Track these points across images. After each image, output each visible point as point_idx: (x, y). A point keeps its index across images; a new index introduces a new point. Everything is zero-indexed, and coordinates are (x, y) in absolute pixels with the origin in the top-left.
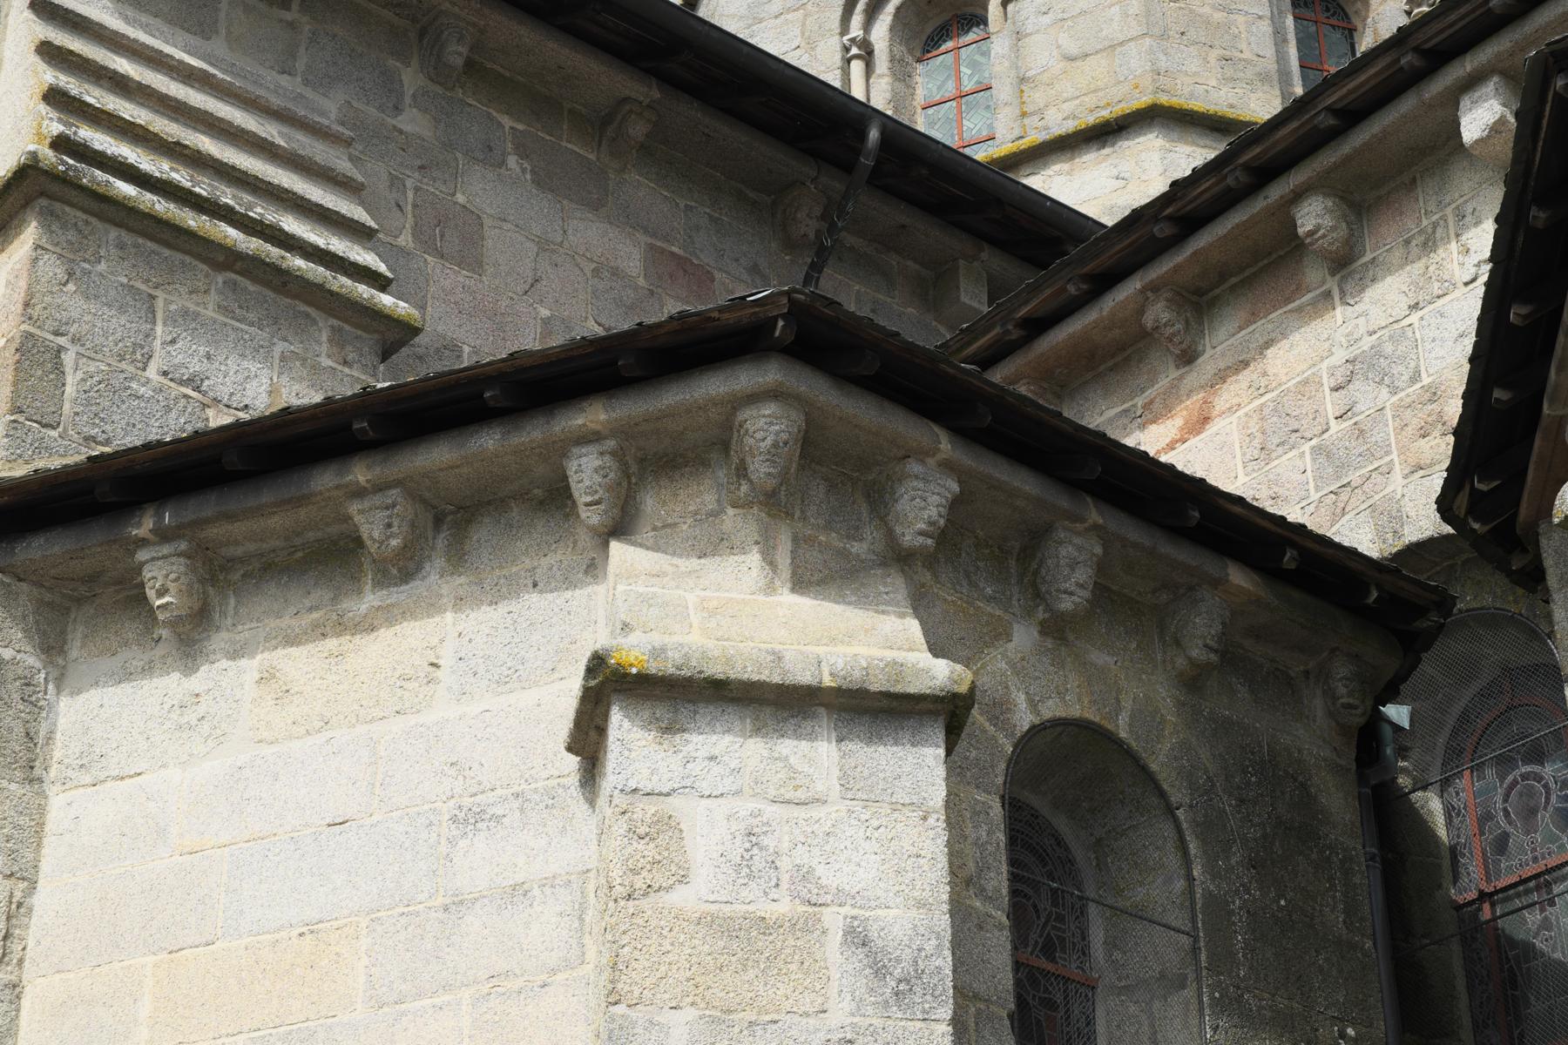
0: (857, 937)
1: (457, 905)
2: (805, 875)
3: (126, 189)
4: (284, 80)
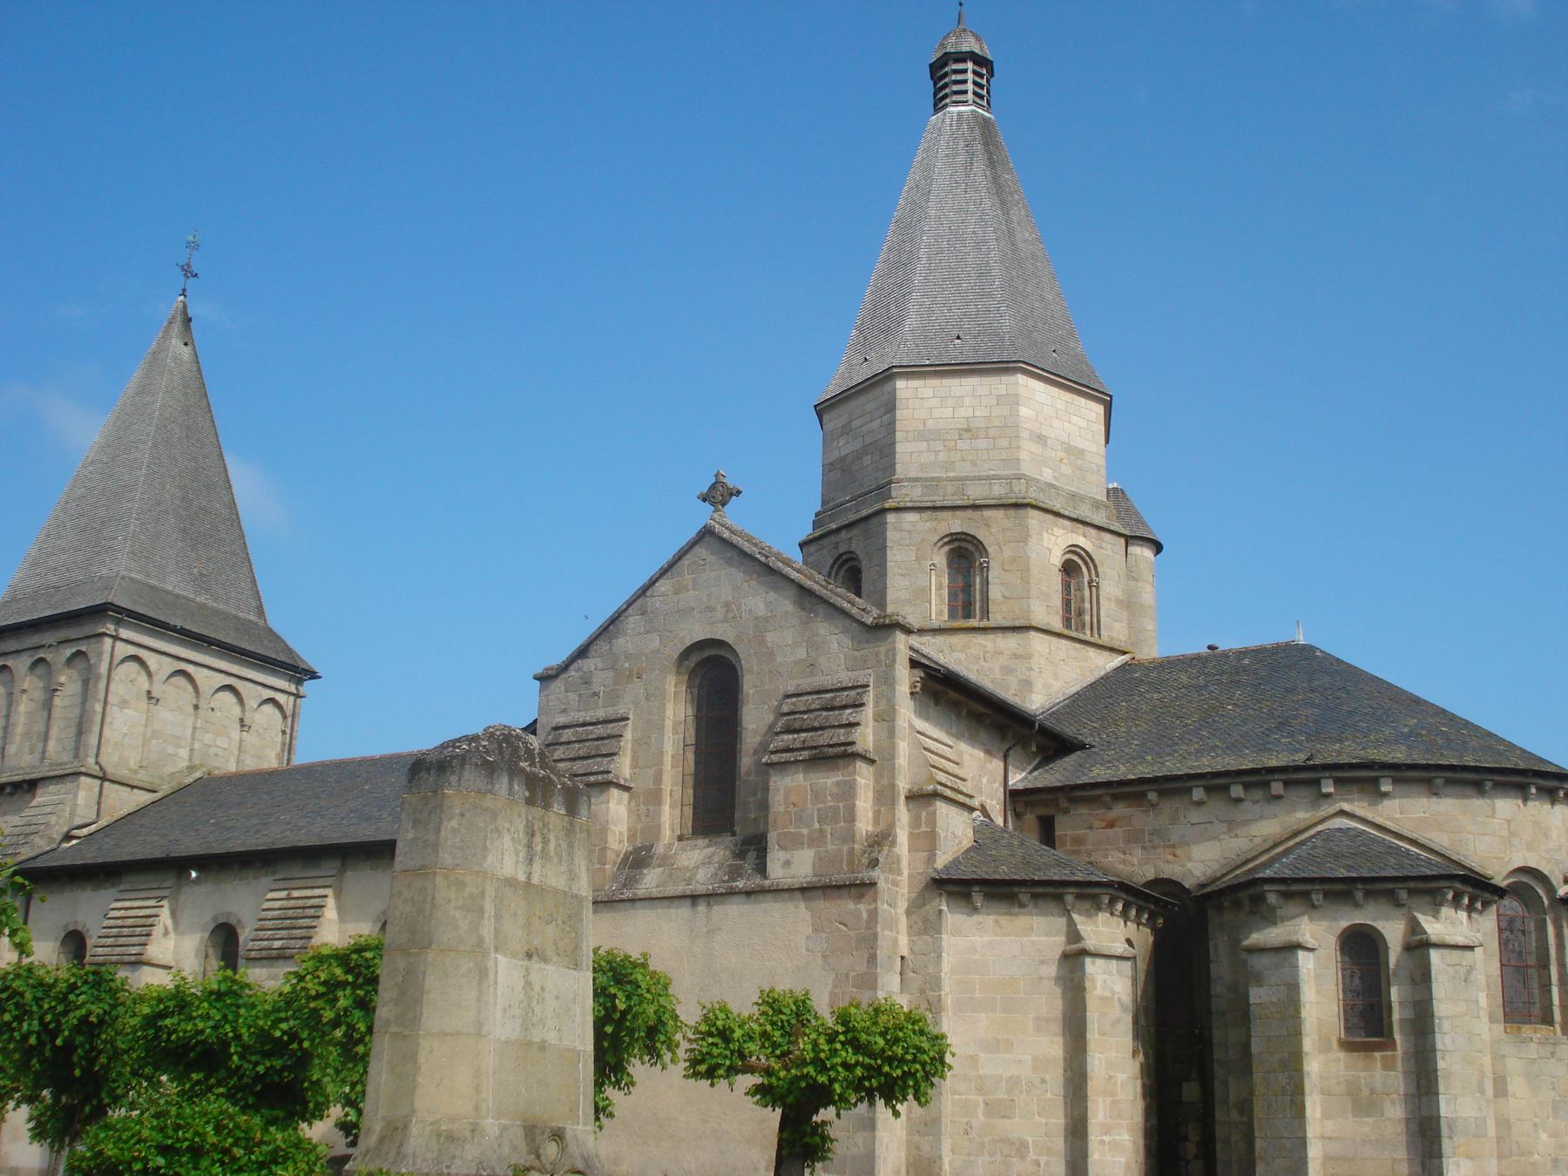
0: (1119, 1000)
1: (1041, 978)
2: (1112, 989)
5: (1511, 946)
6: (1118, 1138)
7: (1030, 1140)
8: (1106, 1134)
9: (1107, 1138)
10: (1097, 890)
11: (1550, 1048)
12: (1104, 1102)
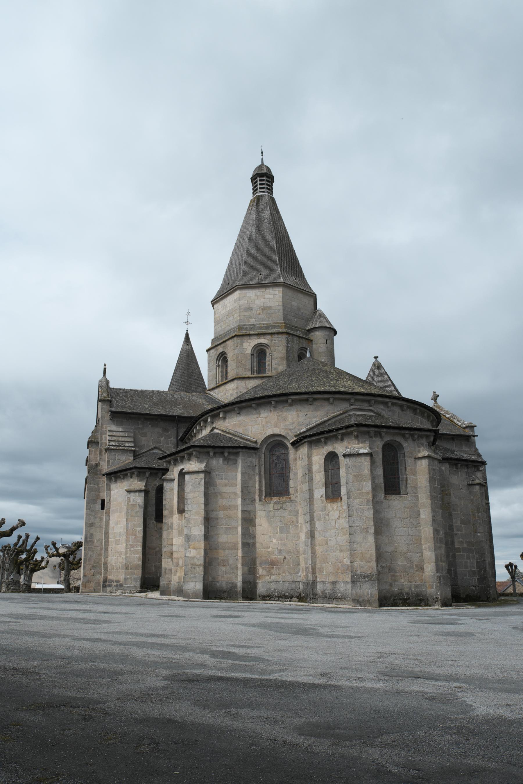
0: (139, 505)
3: (112, 447)
4: (129, 427)
5: (278, 466)
6: (136, 549)
7: (122, 551)
8: (132, 548)
9: (132, 549)
10: (144, 470)
11: (279, 506)
12: (132, 538)
